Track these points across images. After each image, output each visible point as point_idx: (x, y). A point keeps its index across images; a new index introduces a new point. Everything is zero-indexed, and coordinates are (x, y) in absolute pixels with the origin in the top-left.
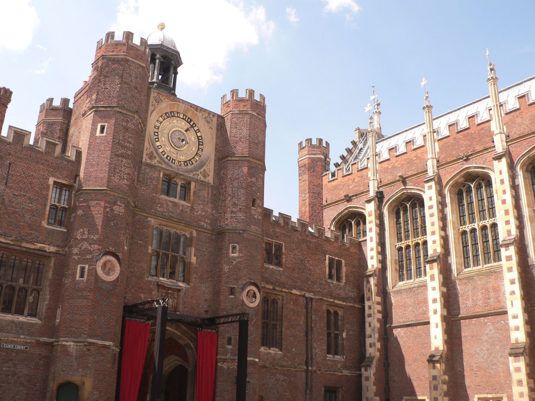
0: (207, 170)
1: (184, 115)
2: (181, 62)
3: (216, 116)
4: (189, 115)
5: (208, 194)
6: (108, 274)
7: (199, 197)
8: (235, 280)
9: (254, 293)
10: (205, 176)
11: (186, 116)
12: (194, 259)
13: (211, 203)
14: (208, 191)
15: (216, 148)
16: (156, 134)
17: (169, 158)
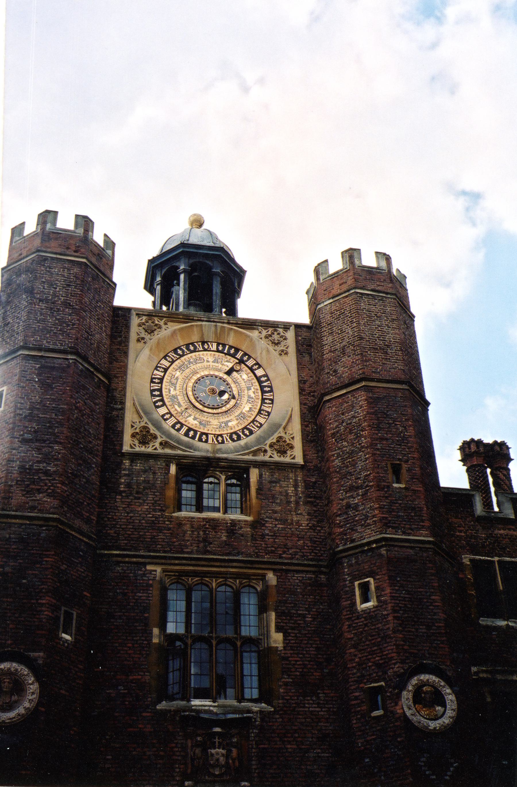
0: (287, 438)
1: (218, 344)
2: (240, 268)
3: (292, 328)
4: (231, 340)
5: (296, 486)
7: (273, 497)
8: (378, 666)
10: (282, 452)
11: (224, 345)
12: (277, 639)
13: (306, 503)
14: (296, 481)
15: (301, 391)
16: (157, 393)
17: (191, 433)
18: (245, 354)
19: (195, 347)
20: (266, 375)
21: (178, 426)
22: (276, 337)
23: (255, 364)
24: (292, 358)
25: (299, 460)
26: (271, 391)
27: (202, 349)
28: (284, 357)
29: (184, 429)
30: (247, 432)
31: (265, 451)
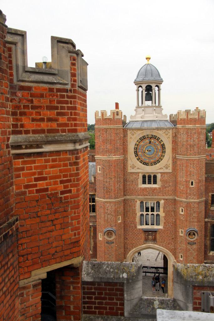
0: (168, 164)
6: (110, 237)
9: (194, 233)
10: (167, 168)
17: (144, 163)
18: (158, 138)
19: (145, 137)
20: (164, 144)
21: (141, 162)
22: (167, 132)
23: (161, 141)
24: (171, 139)
25: (171, 171)
26: (165, 149)
27: (147, 137)
28: (169, 139)
29: (143, 162)
30: (158, 162)
31: (163, 168)
